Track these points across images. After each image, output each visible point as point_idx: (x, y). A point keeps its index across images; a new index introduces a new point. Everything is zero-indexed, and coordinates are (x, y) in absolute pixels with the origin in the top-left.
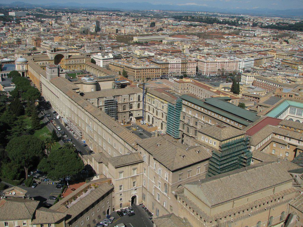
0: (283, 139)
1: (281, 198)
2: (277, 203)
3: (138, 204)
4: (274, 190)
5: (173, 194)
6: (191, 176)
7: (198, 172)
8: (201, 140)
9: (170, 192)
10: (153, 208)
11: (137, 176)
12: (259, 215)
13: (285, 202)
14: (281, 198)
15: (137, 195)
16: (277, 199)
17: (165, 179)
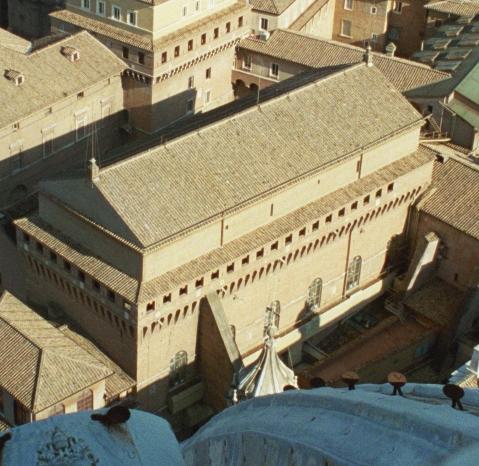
4: (359, 164)
12: (314, 255)
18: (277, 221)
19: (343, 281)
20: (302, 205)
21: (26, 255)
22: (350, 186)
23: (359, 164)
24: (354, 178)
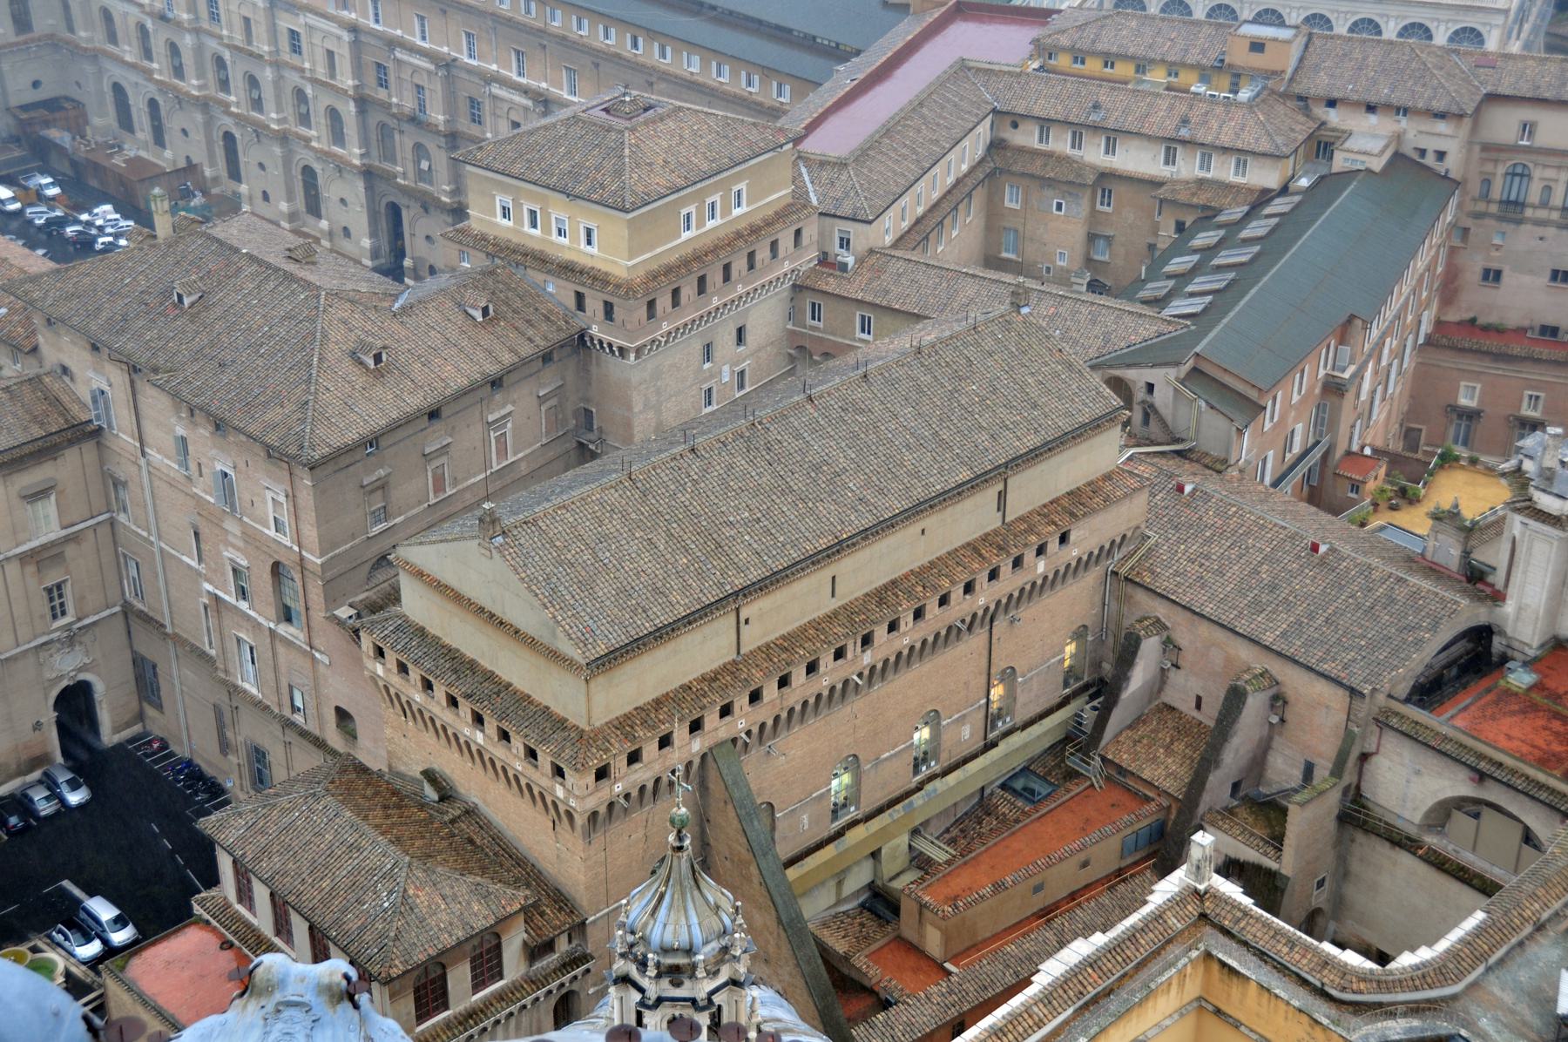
0: (1068, 151)
1: (1053, 545)
2: (1029, 578)
3: (109, 735)
4: (1002, 496)
5: (340, 623)
6: (455, 482)
7: (502, 453)
8: (496, 225)
9: (318, 615)
10: (225, 747)
11: (67, 540)
12: (920, 670)
13: (1082, 565)
14: (1053, 545)
15: (99, 675)
16: (1029, 555)
17: (272, 533)
18: (844, 607)
19: (982, 714)
20: (893, 577)
21: (381, 684)
22: (985, 538)
23: (1002, 496)
24: (993, 522)
